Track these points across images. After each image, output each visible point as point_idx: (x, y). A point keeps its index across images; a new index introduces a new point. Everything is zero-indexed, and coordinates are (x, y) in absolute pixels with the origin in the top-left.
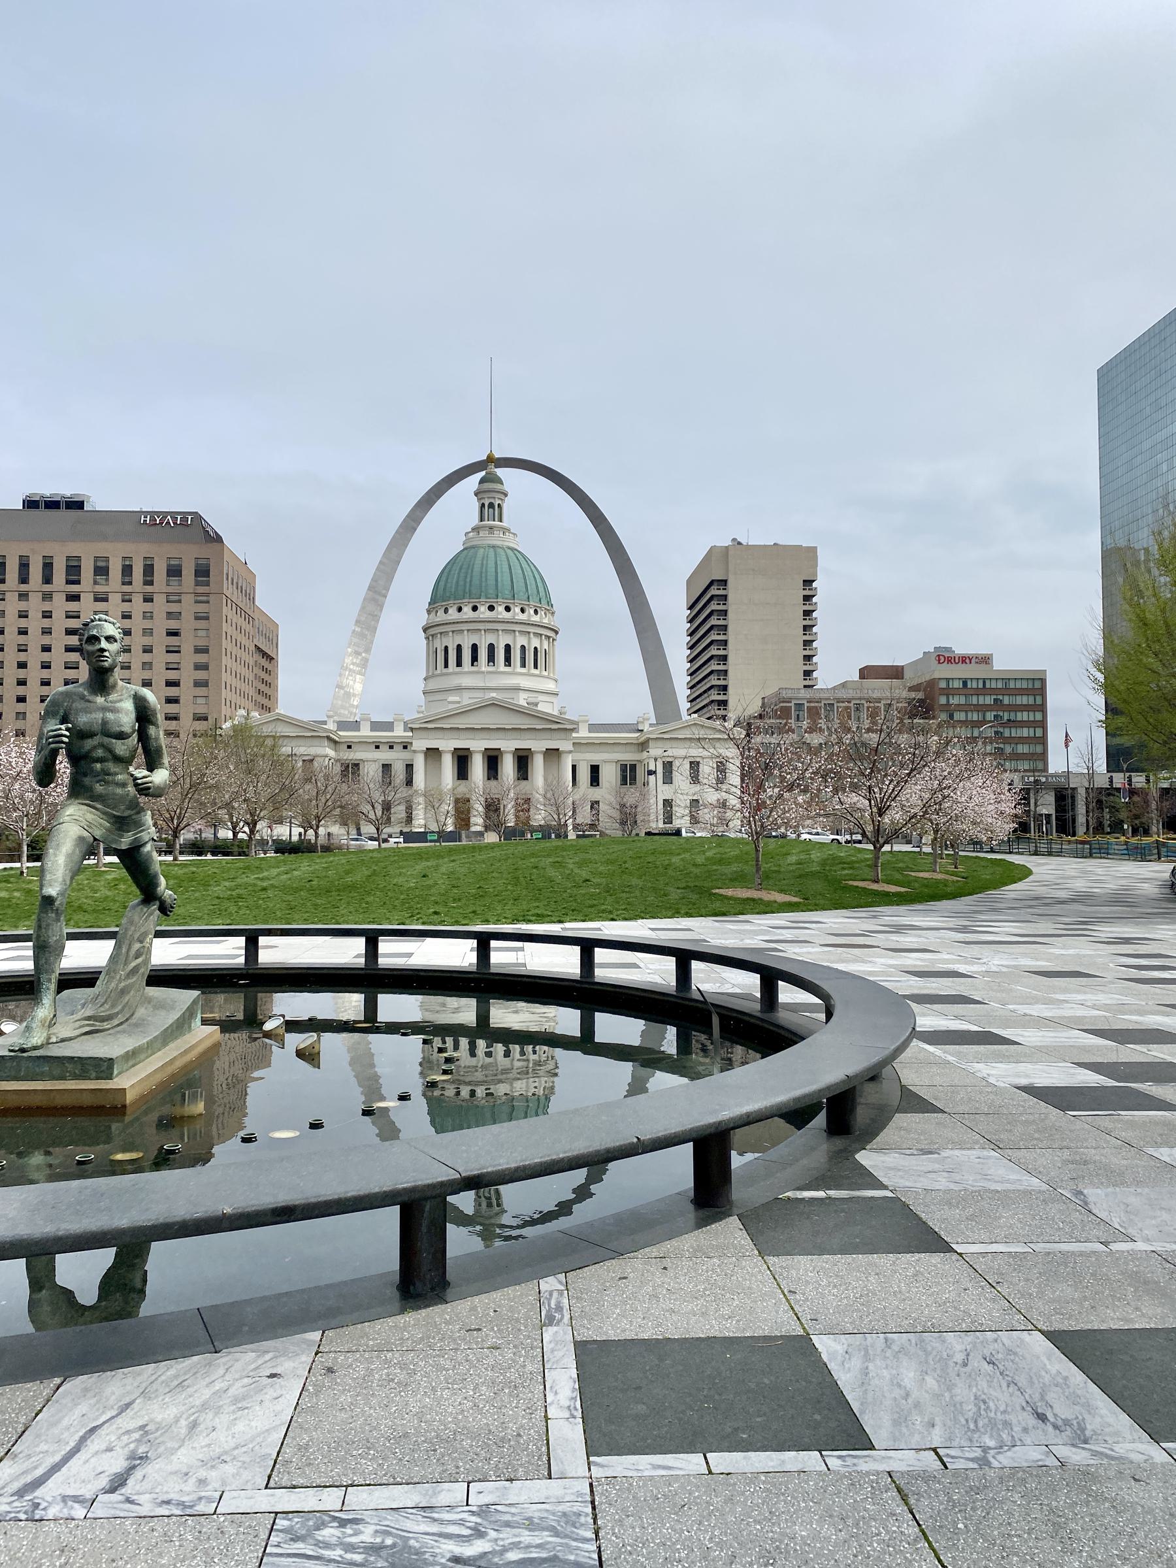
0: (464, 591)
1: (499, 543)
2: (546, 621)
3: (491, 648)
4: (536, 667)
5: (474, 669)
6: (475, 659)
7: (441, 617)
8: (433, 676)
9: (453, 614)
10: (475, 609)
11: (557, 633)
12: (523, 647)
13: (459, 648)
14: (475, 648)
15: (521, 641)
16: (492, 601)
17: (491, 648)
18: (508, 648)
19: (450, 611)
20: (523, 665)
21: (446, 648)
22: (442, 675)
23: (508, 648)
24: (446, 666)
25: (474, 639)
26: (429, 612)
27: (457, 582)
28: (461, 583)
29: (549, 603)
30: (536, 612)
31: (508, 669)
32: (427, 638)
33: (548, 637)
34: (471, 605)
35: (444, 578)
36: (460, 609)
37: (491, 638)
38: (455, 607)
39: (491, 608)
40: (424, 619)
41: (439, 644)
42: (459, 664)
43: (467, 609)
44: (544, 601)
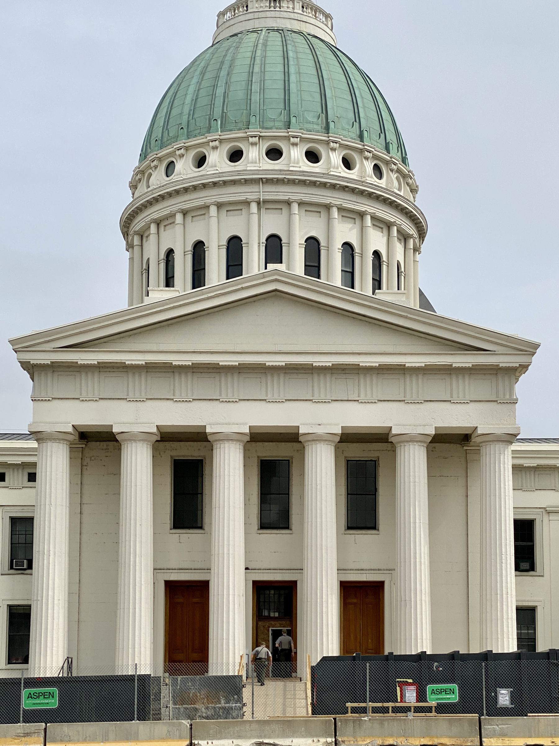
0: (211, 119)
1: (288, 25)
9: (185, 169)
10: (236, 156)
13: (199, 250)
14: (235, 248)
15: (344, 232)
19: (179, 166)
25: (234, 225)
26: (134, 186)
27: (195, 100)
28: (203, 101)
34: (225, 149)
36: (201, 161)
37: (273, 224)
39: (274, 153)
41: (153, 252)
43: (218, 163)
44: (393, 148)
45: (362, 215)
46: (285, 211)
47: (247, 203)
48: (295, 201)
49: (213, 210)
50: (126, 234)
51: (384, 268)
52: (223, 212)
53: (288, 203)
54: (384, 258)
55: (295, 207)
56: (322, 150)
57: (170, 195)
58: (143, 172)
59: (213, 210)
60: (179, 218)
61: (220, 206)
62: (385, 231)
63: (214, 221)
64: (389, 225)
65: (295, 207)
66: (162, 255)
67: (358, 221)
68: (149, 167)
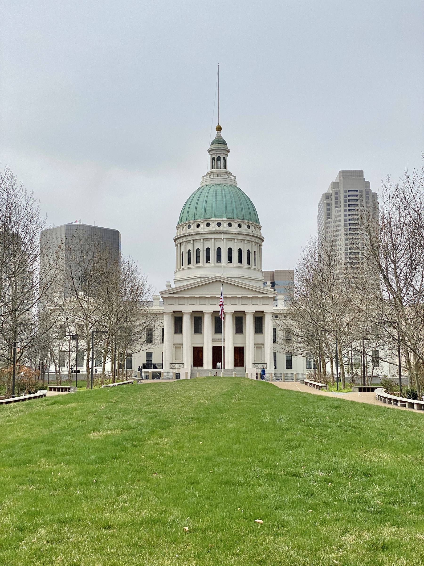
2: (255, 233)
3: (219, 250)
4: (249, 263)
6: (208, 259)
7: (186, 231)
8: (181, 270)
10: (208, 225)
11: (263, 241)
12: (240, 250)
14: (208, 250)
16: (219, 220)
17: (219, 250)
18: (230, 251)
19: (192, 226)
20: (240, 261)
21: (189, 251)
22: (186, 269)
24: (189, 263)
26: (178, 228)
29: (257, 221)
30: (249, 227)
31: (230, 264)
32: (177, 245)
35: (187, 206)
36: (198, 226)
38: (196, 224)
39: (219, 224)
40: (174, 233)
42: (198, 262)
47: (211, 239)
51: (251, 254)
55: (225, 240)
56: (232, 223)
58: (181, 225)
59: (202, 240)
61: (204, 239)
62: (251, 243)
64: (252, 242)
65: (225, 240)
68: (183, 225)
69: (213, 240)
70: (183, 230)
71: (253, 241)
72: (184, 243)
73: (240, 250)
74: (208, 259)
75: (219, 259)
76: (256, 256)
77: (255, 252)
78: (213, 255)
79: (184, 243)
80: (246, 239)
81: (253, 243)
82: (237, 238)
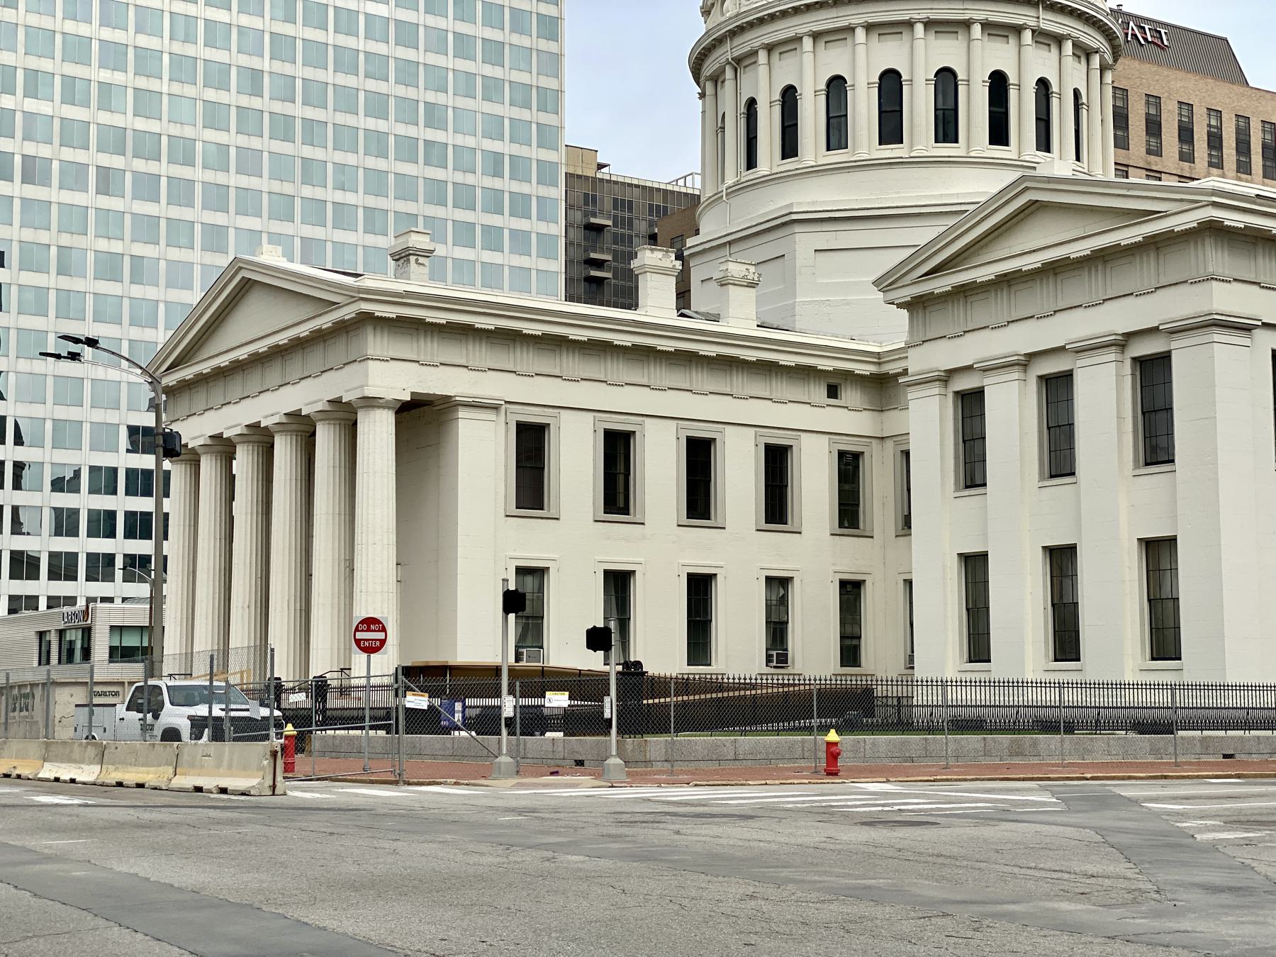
3: (891, 84)
5: (838, 156)
6: (837, 134)
12: (998, 83)
13: (789, 97)
17: (891, 84)
18: (946, 79)
20: (999, 135)
21: (752, 103)
22: (739, 189)
23: (946, 79)
24: (751, 163)
26: (706, 12)
31: (946, 150)
33: (1084, 52)
42: (789, 148)
45: (1018, 30)
46: (906, 36)
47: (851, 29)
48: (920, 21)
49: (808, 43)
50: (698, 84)
51: (1055, 102)
52: (821, 44)
53: (910, 24)
54: (1055, 88)
55: (919, 28)
57: (751, 25)
59: (808, 43)
60: (762, 56)
61: (816, 36)
62: (1054, 50)
63: (808, 58)
64: (1059, 40)
65: (919, 28)
66: (743, 109)
67: (1013, 41)
69: (860, 33)
70: (723, 14)
71: (1068, 37)
72: (729, 73)
73: (998, 83)
74: (837, 134)
75: (891, 129)
76: (1084, 113)
77: (1077, 93)
78: (864, 108)
79: (729, 73)
80: (1032, 23)
81: (1068, 47)
82: (981, 16)
